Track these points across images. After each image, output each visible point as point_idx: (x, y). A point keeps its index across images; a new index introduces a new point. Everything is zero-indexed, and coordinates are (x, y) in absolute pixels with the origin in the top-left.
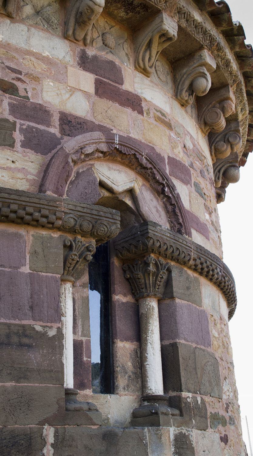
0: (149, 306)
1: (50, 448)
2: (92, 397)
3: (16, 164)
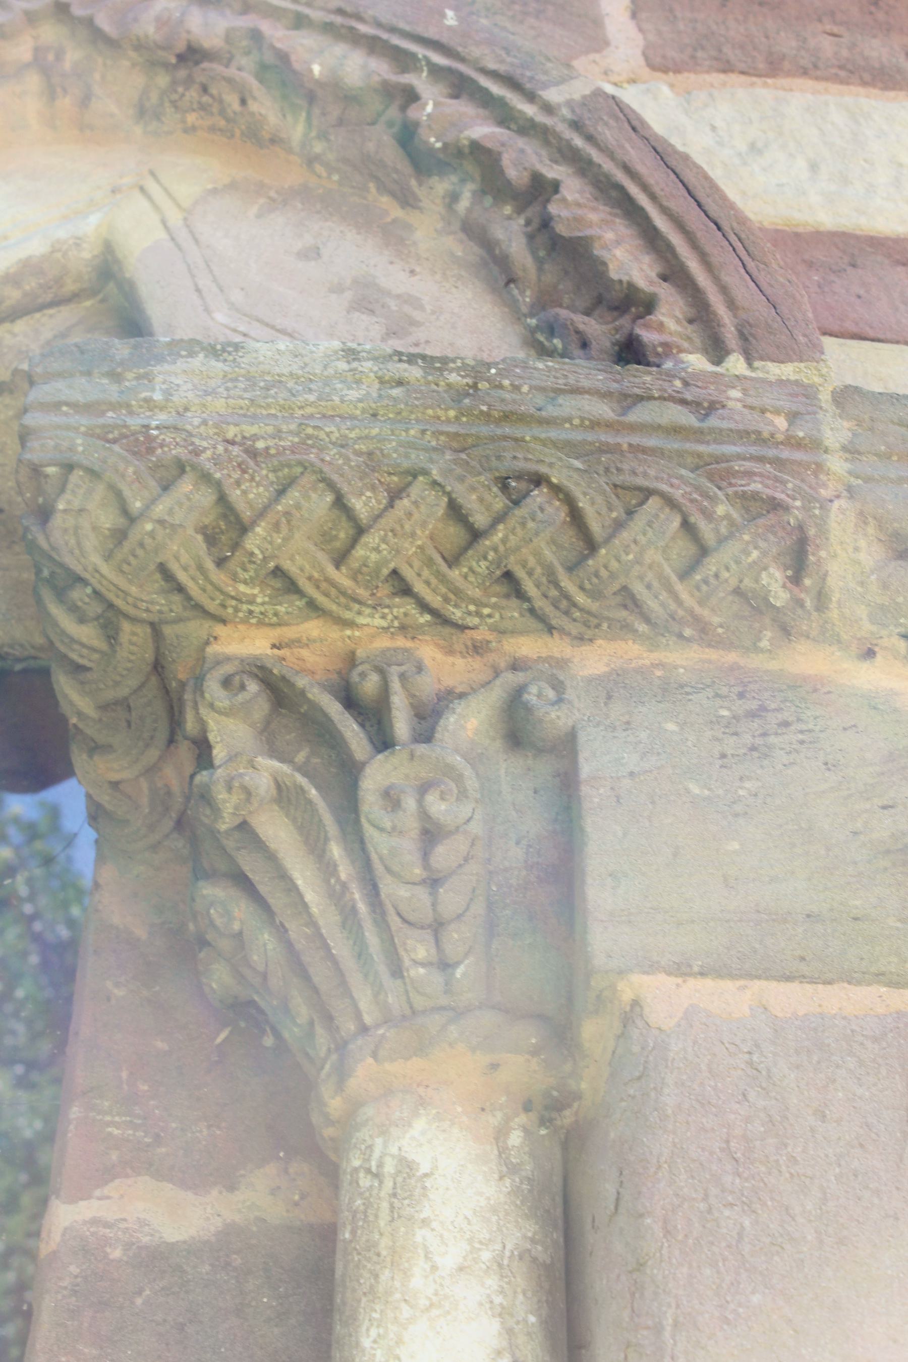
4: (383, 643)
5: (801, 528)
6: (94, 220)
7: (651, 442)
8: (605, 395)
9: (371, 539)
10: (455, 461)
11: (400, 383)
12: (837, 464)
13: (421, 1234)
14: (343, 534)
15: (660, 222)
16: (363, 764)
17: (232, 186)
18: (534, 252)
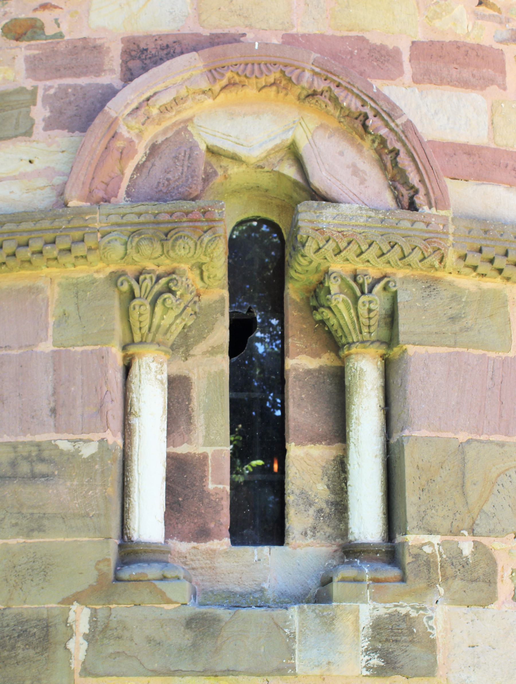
1: (82, 640)
4: (362, 268)
5: (443, 254)
6: (291, 133)
7: (417, 234)
8: (409, 220)
11: (370, 217)
12: (451, 238)
14: (359, 252)
16: (359, 298)
17: (322, 126)
18: (392, 164)
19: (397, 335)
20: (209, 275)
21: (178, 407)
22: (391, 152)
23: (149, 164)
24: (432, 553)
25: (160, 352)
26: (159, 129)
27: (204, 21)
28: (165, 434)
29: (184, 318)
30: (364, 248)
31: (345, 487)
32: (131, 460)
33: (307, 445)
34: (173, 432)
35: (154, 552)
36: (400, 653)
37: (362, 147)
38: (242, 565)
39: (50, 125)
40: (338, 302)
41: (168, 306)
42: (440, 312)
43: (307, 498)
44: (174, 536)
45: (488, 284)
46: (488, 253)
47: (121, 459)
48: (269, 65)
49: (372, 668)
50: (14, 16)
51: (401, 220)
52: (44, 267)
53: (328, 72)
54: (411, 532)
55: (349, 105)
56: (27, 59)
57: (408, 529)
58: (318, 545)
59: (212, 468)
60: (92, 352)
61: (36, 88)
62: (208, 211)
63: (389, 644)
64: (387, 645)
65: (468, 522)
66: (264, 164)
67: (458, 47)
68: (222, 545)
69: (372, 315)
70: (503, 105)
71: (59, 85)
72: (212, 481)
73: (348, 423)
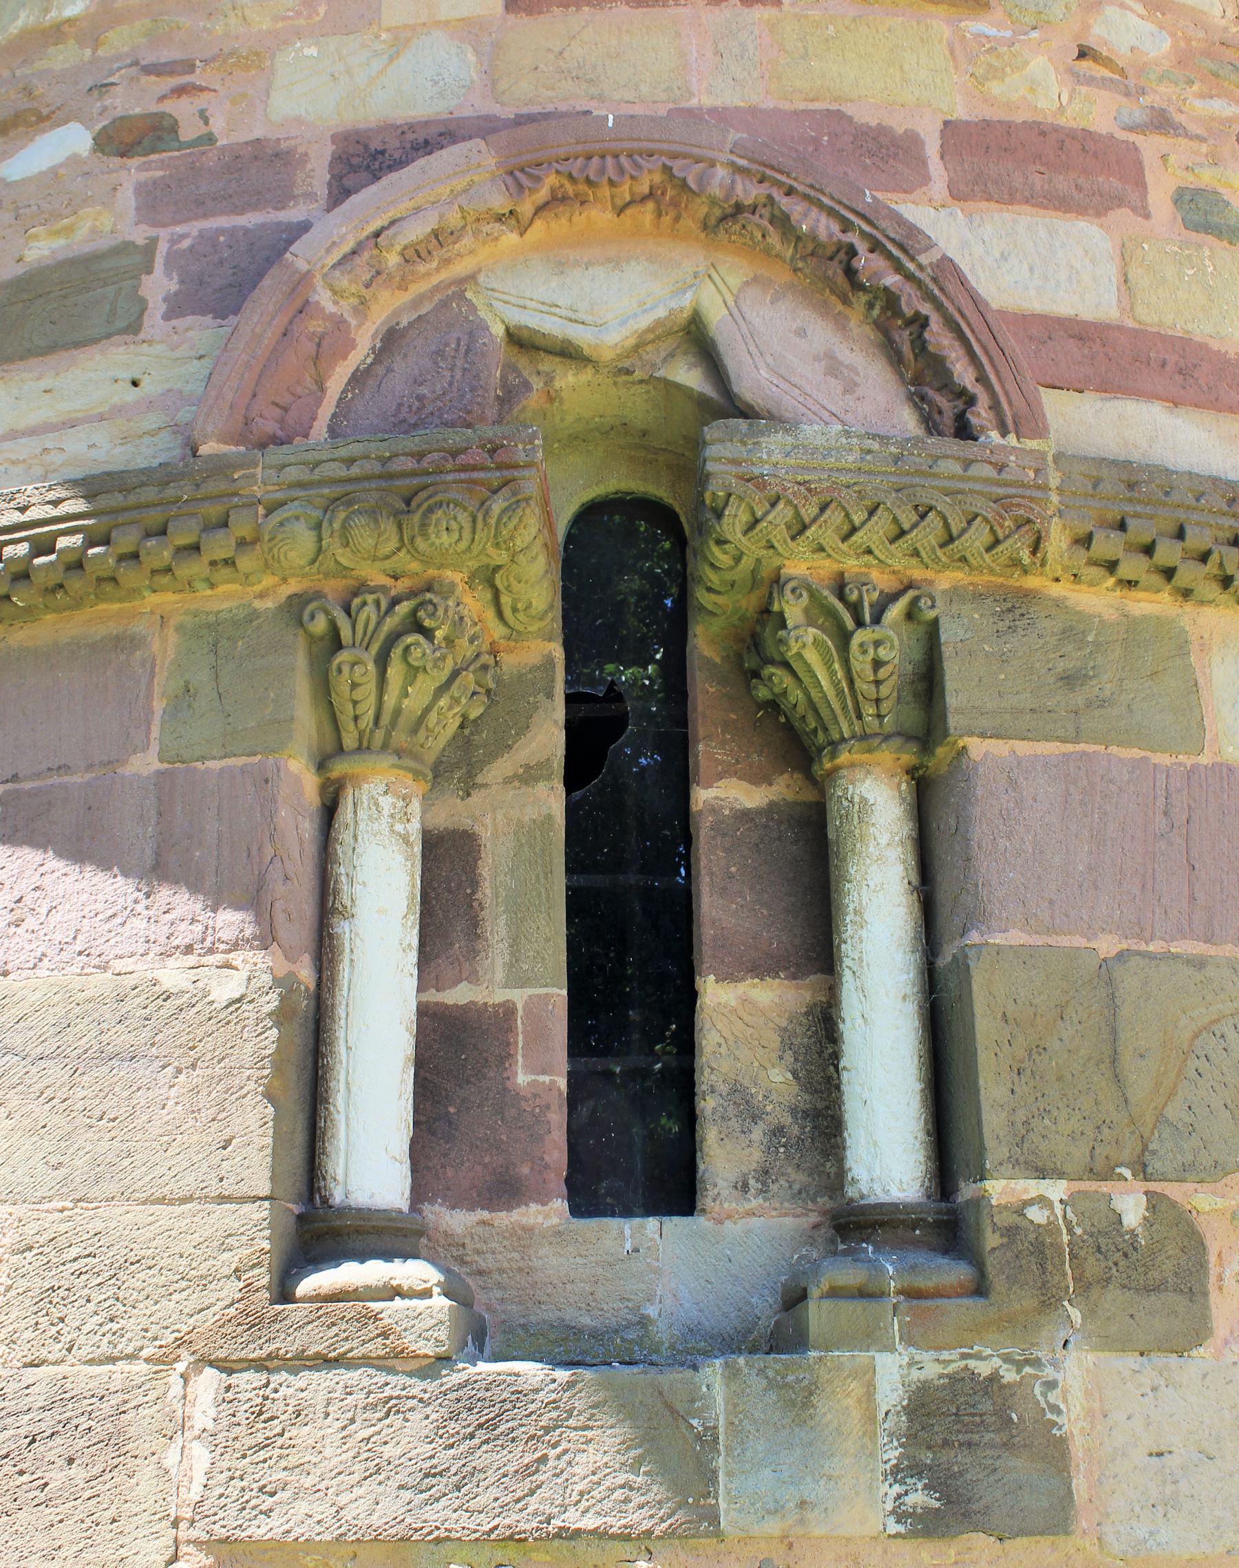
0: (845, 803)
2: (559, 1233)
3: (142, 384)
4: (856, 570)
5: (1039, 532)
6: (689, 295)
7: (978, 487)
8: (958, 459)
9: (860, 534)
10: (897, 498)
11: (869, 452)
12: (1055, 498)
13: (872, 829)
14: (846, 528)
15: (977, 348)
16: (852, 633)
17: (756, 279)
18: (913, 350)
19: (944, 717)
20: (515, 601)
21: (447, 901)
22: (909, 322)
23: (380, 370)
24: (1049, 1223)
25: (402, 772)
26: (405, 297)
27: (503, 93)
28: (413, 957)
29: (456, 695)
30: (857, 519)
31: (835, 1075)
32: (332, 1018)
33: (743, 979)
34: (437, 957)
35: (378, 1231)
36: (980, 1476)
37: (847, 318)
38: (596, 1263)
39: (176, 308)
40: (804, 646)
41: (415, 664)
42: (1038, 665)
43: (747, 1102)
44: (436, 1196)
45: (1143, 604)
46: (1140, 531)
47: (311, 1015)
48: (637, 157)
49: (911, 1515)
50: (119, 112)
51: (938, 457)
52: (146, 594)
53: (765, 166)
54: (995, 1174)
55: (813, 230)
56: (140, 189)
57: (988, 1166)
58: (774, 1213)
59: (525, 1038)
60: (243, 770)
61: (153, 241)
62: (503, 446)
63: (952, 1454)
64: (946, 1456)
65: (1130, 1149)
66: (633, 365)
67: (1043, 134)
68: (547, 1216)
69: (883, 673)
70: (1145, 246)
71: (200, 231)
72: (525, 1066)
73: (838, 926)
